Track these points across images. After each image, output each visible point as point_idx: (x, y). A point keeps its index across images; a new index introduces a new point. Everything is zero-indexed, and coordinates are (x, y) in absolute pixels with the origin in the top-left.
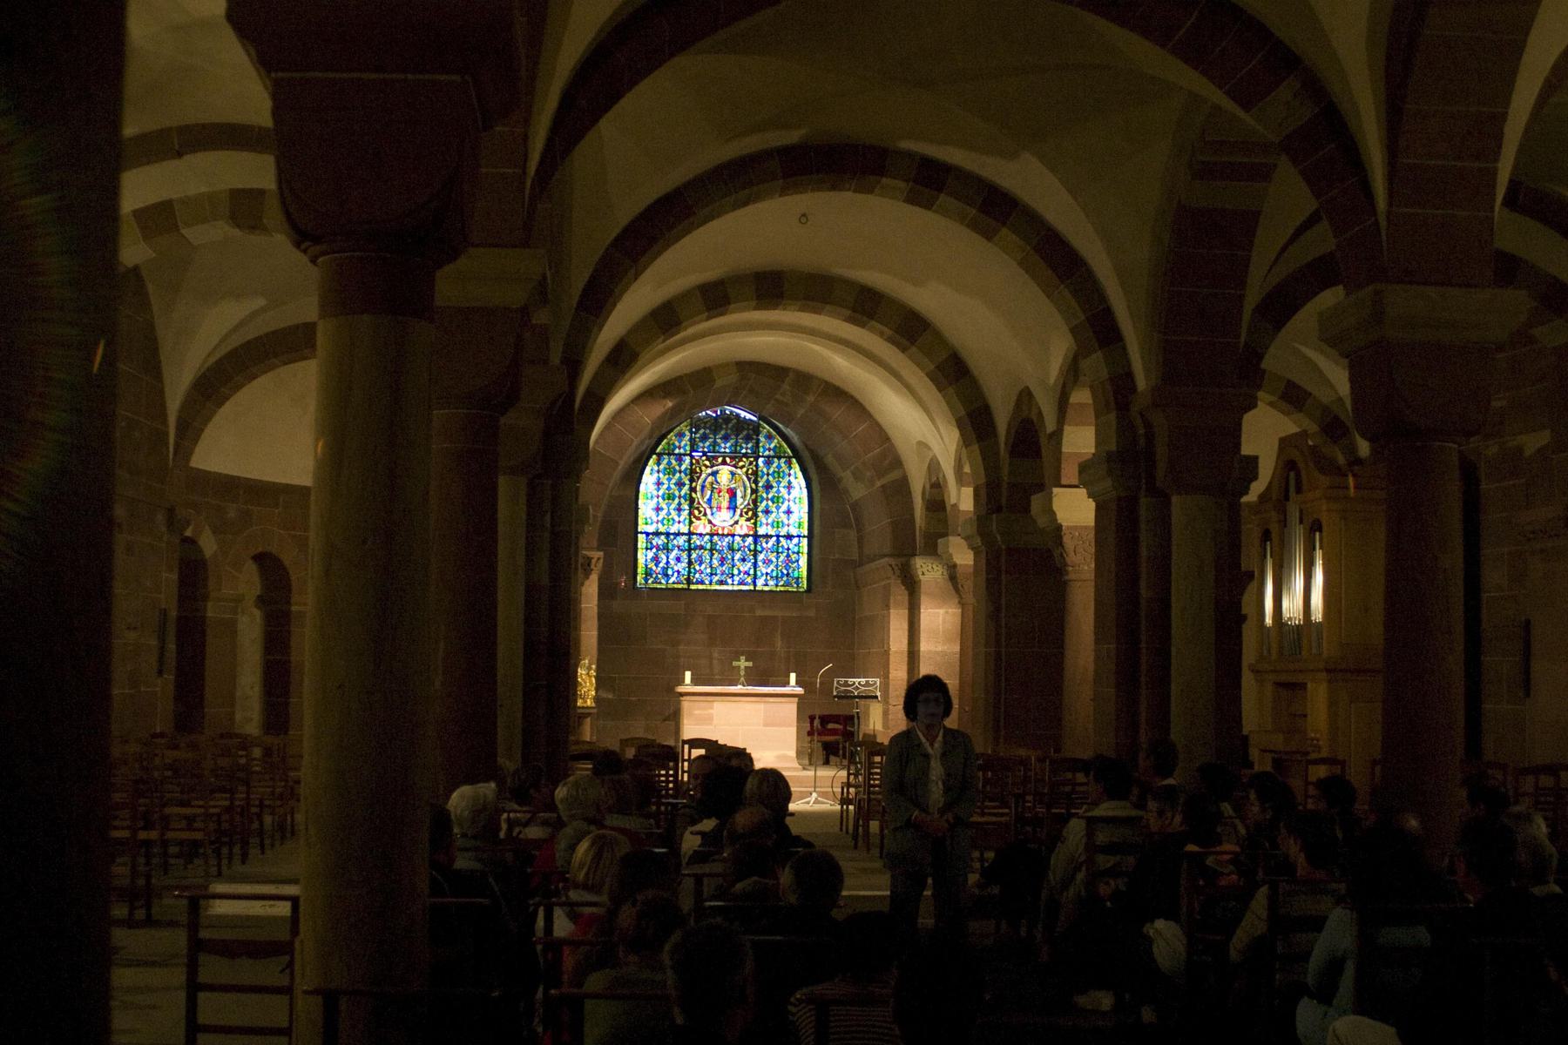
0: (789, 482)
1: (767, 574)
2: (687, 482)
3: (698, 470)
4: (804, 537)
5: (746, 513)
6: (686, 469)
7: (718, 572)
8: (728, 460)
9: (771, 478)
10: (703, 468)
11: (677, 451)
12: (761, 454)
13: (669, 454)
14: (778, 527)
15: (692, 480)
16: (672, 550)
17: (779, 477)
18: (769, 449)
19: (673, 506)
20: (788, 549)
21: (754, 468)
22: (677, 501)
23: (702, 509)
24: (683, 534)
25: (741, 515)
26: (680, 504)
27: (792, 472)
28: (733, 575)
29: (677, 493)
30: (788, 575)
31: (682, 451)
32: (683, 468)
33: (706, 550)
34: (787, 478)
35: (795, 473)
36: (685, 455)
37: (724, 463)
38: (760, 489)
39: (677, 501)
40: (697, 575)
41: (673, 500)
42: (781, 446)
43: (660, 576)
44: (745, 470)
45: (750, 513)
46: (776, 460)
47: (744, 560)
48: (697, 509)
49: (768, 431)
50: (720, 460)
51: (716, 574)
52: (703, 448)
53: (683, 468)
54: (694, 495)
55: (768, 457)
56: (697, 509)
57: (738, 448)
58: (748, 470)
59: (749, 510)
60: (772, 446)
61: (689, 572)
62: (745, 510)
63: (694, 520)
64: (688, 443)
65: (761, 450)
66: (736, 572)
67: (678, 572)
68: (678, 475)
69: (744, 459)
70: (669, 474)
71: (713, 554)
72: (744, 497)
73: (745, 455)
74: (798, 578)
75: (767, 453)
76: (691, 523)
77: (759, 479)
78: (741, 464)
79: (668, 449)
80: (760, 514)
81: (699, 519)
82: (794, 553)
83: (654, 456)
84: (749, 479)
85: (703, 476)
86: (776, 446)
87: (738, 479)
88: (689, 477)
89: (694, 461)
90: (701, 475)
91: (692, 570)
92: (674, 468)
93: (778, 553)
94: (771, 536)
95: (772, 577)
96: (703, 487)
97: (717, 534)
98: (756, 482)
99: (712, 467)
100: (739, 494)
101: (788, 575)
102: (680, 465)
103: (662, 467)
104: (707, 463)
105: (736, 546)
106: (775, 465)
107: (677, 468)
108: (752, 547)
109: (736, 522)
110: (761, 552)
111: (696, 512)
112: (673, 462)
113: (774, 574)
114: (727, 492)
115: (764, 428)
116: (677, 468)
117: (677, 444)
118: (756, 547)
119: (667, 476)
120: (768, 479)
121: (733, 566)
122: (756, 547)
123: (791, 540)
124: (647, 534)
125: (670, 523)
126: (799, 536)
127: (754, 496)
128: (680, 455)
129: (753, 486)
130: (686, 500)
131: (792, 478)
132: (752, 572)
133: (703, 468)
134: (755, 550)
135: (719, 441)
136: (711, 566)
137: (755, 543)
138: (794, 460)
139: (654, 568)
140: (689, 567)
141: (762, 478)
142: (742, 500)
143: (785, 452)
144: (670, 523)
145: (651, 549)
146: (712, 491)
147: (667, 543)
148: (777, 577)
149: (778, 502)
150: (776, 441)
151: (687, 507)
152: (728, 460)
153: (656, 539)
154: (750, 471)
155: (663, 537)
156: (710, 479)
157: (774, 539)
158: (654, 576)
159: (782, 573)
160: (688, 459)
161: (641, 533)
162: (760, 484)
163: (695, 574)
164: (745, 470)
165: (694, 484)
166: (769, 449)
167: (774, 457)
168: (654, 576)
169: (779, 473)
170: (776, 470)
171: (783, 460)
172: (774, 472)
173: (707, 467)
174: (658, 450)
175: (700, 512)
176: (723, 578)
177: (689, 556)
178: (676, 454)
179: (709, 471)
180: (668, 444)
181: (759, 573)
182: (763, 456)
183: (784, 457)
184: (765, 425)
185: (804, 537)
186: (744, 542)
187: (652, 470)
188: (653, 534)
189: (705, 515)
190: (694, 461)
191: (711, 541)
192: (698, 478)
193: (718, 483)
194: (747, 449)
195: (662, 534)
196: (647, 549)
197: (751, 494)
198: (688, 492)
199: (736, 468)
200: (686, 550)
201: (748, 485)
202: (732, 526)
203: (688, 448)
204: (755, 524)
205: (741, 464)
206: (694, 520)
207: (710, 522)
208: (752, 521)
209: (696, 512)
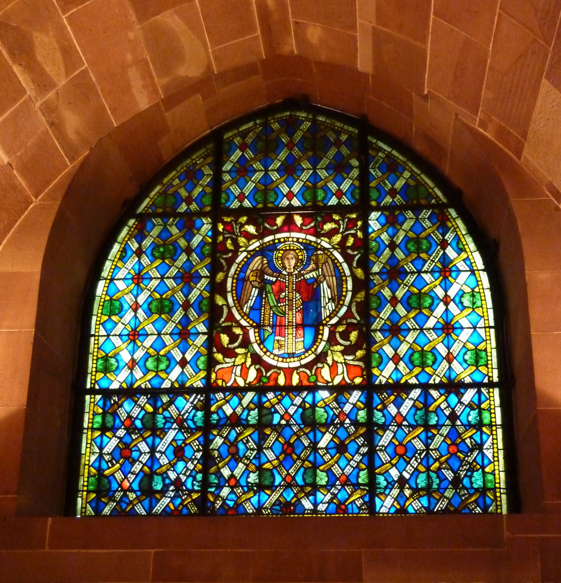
0: (445, 261)
1: (402, 481)
2: (205, 272)
3: (229, 244)
4: (491, 385)
5: (345, 335)
6: (203, 243)
7: (278, 480)
8: (298, 220)
9: (400, 254)
10: (242, 241)
11: (183, 208)
12: (373, 203)
13: (165, 216)
14: (423, 365)
15: (215, 268)
16: (164, 431)
17: (419, 250)
18: (393, 193)
19: (170, 327)
20: (453, 417)
21: (360, 234)
22: (179, 315)
23: (238, 331)
24: (192, 390)
25: (332, 341)
26: (185, 321)
27: (449, 237)
28: (315, 488)
29: (180, 297)
30: (456, 482)
31: (194, 207)
32: (196, 241)
33: (247, 426)
34: (437, 253)
35: (458, 239)
36: (201, 214)
37: (289, 225)
38: (377, 279)
39: (179, 315)
40: (225, 491)
41: (171, 312)
42: (419, 184)
43: (132, 496)
44: (337, 238)
45: (354, 336)
46: (410, 214)
47: (341, 448)
48: (228, 331)
49: (389, 155)
50: (279, 221)
51: (272, 487)
52: (241, 197)
53: (196, 241)
54: (220, 301)
55: (391, 208)
56: (228, 331)
57: (321, 194)
58: (345, 239)
59: (351, 327)
60: (399, 184)
61: (205, 484)
62: (341, 329)
63: (219, 357)
64: (208, 190)
65: (374, 194)
66: (322, 479)
67: (178, 483)
68: (183, 257)
69: (336, 217)
70: (163, 258)
71: (263, 438)
72: (337, 299)
73: (340, 209)
74: (483, 491)
75: (388, 200)
76: (211, 363)
77: (372, 258)
78: (328, 226)
79: (164, 206)
80: (379, 336)
81: (229, 353)
82: (469, 426)
83: (132, 222)
84: (348, 259)
85: (242, 256)
86: (406, 185)
87: (322, 258)
88: (208, 261)
89: (221, 227)
90: (236, 256)
91: (213, 479)
92: (175, 243)
93: (427, 427)
94: (408, 387)
95: (416, 491)
96: (241, 281)
97: (276, 388)
98: (365, 264)
99: (260, 237)
100: (326, 292)
101: (456, 482)
102: (189, 237)
103: (147, 243)
104: (251, 229)
105: (321, 414)
106: (407, 226)
107: (182, 243)
108: (362, 415)
109: (321, 358)
110: (384, 427)
111: (225, 339)
112: (174, 230)
113: (422, 481)
114: (298, 290)
115: (381, 150)
116: (182, 243)
117: (183, 193)
118: (370, 415)
119: (158, 262)
120: (393, 256)
121: (315, 466)
122: (370, 415)
123: (460, 395)
124: (107, 393)
125: (162, 366)
126: (477, 385)
127: (361, 296)
128: (189, 214)
129: (359, 272)
130: (200, 313)
131: (451, 252)
132: (363, 477)
133: (242, 241)
134: (370, 423)
135: (275, 176)
136: (260, 468)
137: (369, 406)
138: (453, 212)
139: (119, 476)
140: (205, 472)
141: (378, 254)
142: (331, 306)
143: (430, 196)
144: (162, 366)
145: (114, 429)
146: (262, 290)
147: (155, 411)
148: (428, 490)
149: (420, 307)
150: (407, 174)
151: (202, 328)
152: (298, 220)
153: (127, 406)
154: (351, 241)
155: (143, 400)
156: (256, 263)
157: (416, 393)
158: (118, 495)
159: (442, 479)
160: (206, 227)
161: (93, 392)
162: (376, 269)
163: (219, 487)
164: (337, 238)
165: (220, 276)
166: (393, 193)
167: (403, 208)
168: (118, 495)
169: (417, 241)
170: (411, 234)
171: (426, 214)
172: (407, 239)
173: (249, 237)
174: (140, 210)
175: (233, 338)
176: (289, 496)
177: (207, 442)
178: (180, 214)
179: (255, 245)
180: (163, 194)
181: (381, 481)
182: (377, 209)
183: (428, 207)
184: (381, 144)
185: (491, 385)
186: (341, 404)
187: (124, 251)
188: (120, 392)
189: (246, 343)
190: (221, 227)
191: (260, 406)
192: (230, 262)
193: (275, 270)
194: (339, 194)
195: (141, 391)
196: (104, 429)
197: (355, 292)
198: (206, 294)
199: (318, 235)
200: (198, 429)
201: (347, 272)
202: (309, 366)
203: (207, 200)
204: (367, 359)
205: (328, 226)
206: (219, 357)
207: (257, 359)
208: (359, 353)
209: (225, 339)
